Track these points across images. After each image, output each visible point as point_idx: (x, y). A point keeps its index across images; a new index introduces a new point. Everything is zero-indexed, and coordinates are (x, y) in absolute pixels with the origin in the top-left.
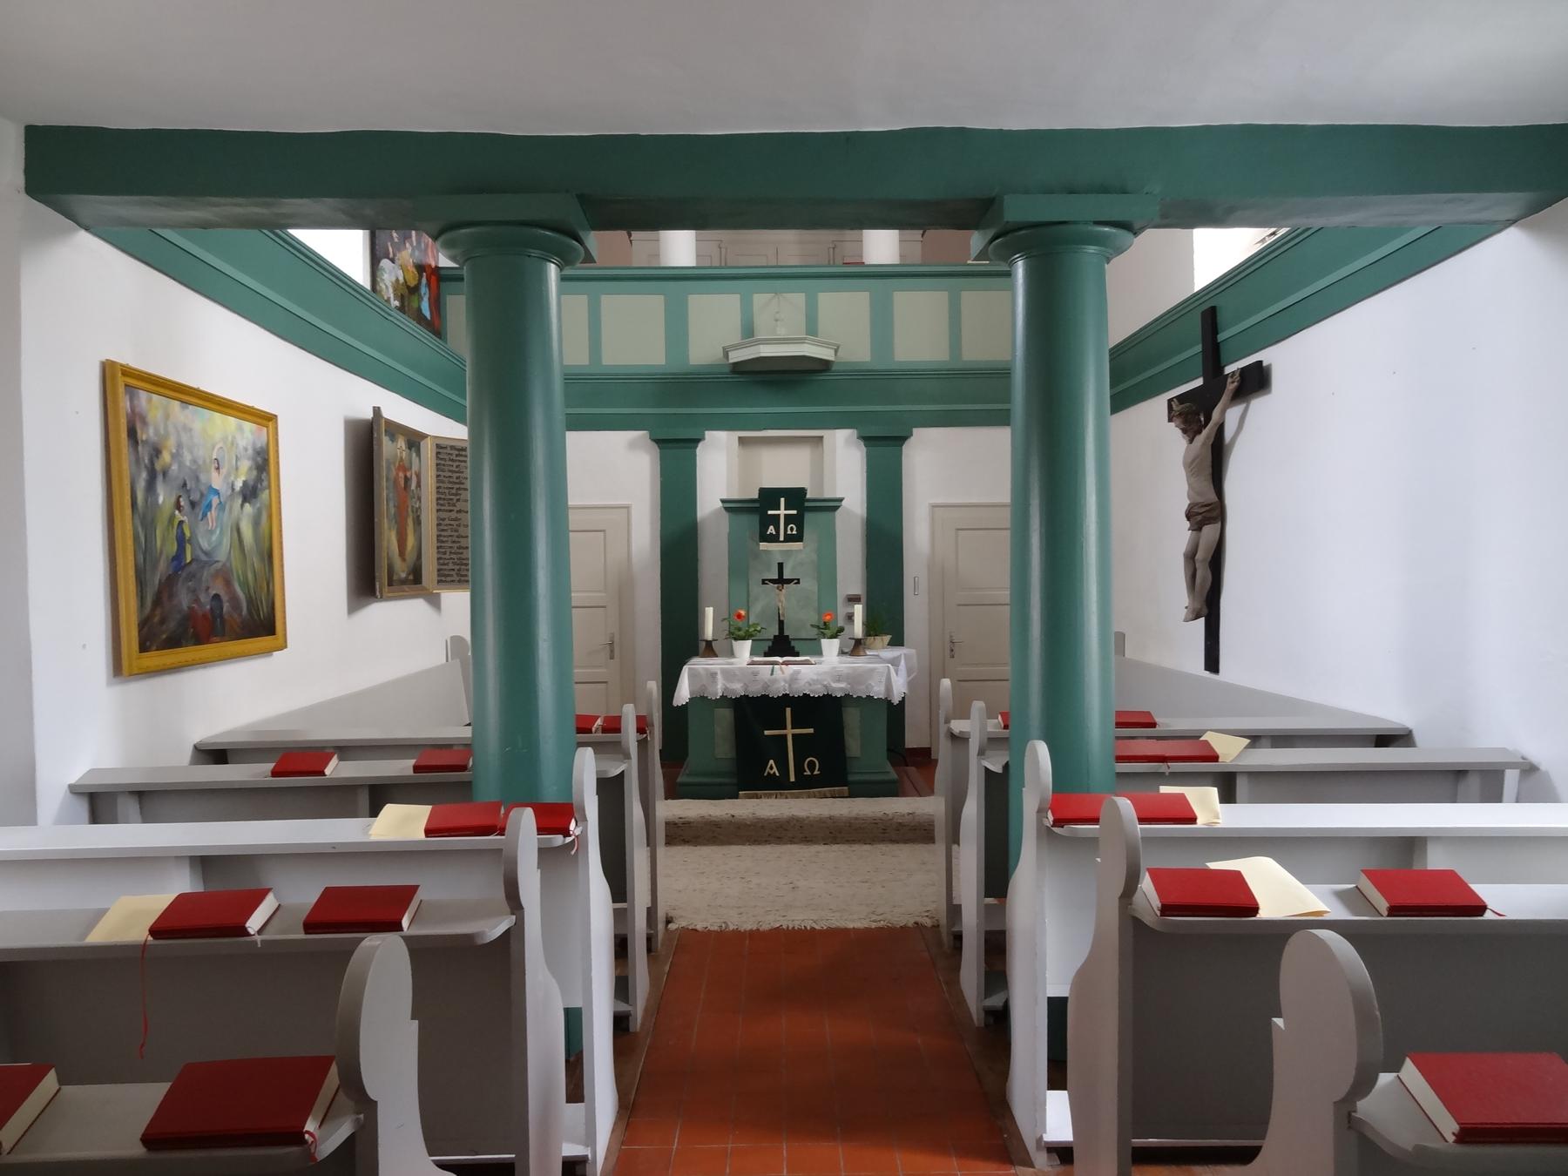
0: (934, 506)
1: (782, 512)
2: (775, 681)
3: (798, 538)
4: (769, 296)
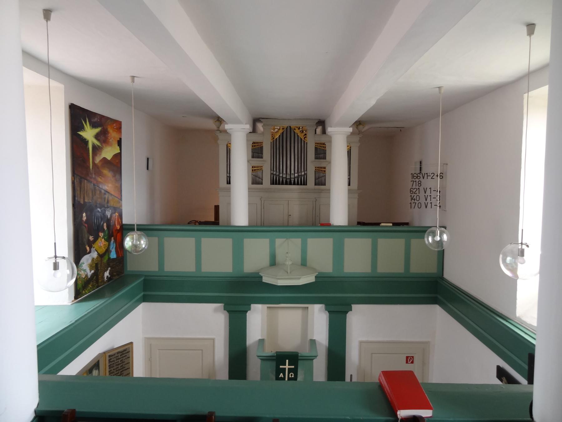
1: (287, 367)
4: (285, 239)
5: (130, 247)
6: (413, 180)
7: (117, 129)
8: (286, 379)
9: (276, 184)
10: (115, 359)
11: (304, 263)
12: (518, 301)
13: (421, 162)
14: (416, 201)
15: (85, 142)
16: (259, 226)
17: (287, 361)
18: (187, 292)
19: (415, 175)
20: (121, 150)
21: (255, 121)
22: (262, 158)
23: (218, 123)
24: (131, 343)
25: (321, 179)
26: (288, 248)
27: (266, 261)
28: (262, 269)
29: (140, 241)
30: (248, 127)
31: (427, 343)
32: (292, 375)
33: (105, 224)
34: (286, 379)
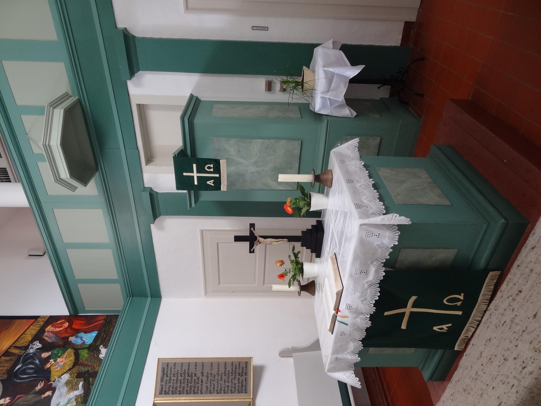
0: (187, 8)
1: (195, 175)
2: (354, 325)
8: (217, 175)
10: (168, 385)
17: (185, 174)
34: (217, 175)
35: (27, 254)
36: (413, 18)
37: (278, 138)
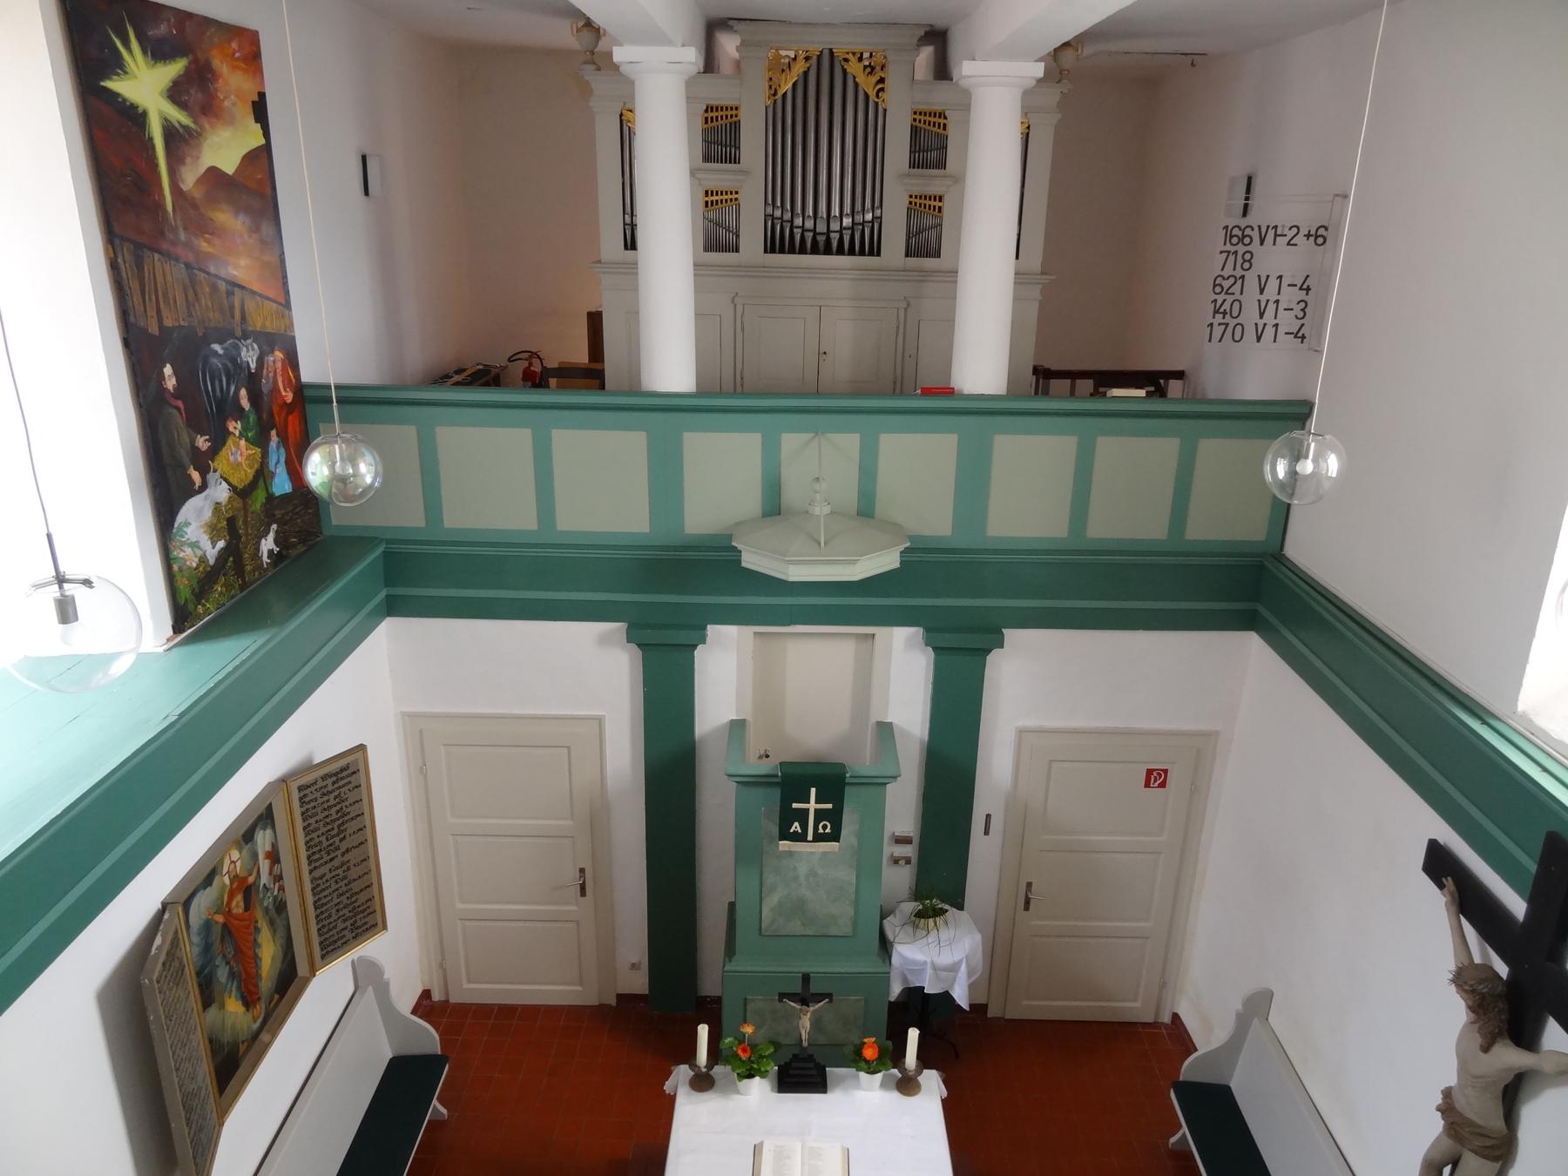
1: (812, 806)
3: (835, 836)
5: (322, 484)
6: (1228, 247)
7: (245, 59)
8: (810, 837)
9: (782, 251)
11: (866, 510)
12: (1530, 669)
13: (1250, 179)
14: (1228, 319)
15: (134, 117)
16: (730, 392)
18: (515, 588)
19: (1236, 231)
20: (267, 134)
21: (713, 27)
22: (736, 161)
23: (587, 36)
24: (361, 748)
25: (927, 238)
26: (820, 461)
27: (750, 502)
28: (738, 524)
29: (355, 466)
30: (691, 56)
31: (1209, 736)
32: (825, 827)
33: (243, 392)
34: (810, 837)
35: (367, 152)
36: (992, 1012)
37: (856, 903)
